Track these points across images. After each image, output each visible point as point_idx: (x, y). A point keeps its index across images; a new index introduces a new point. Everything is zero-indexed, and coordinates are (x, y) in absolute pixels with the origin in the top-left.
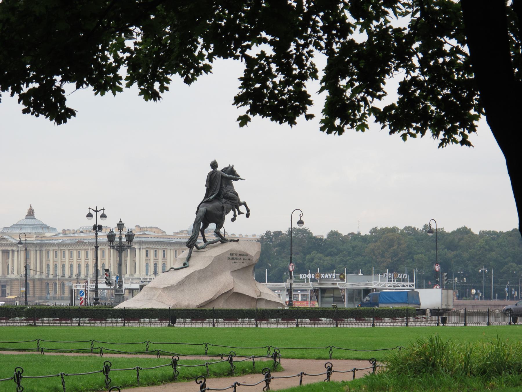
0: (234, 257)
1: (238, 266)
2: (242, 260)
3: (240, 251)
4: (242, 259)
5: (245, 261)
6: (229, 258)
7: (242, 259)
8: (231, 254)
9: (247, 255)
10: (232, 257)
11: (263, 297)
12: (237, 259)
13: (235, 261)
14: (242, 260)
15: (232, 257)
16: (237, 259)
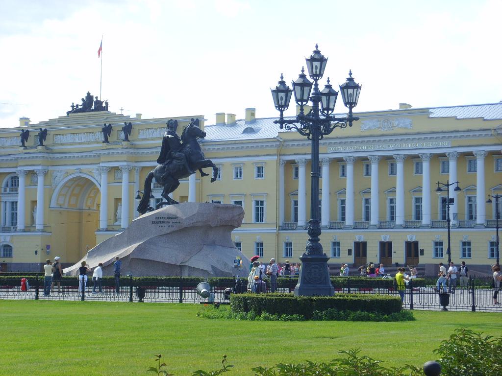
0: (162, 220)
1: (166, 230)
2: (171, 224)
3: (168, 214)
4: (171, 222)
5: (174, 224)
6: (153, 222)
7: (171, 222)
8: (157, 218)
9: (176, 218)
10: (158, 220)
11: (187, 264)
12: (164, 222)
13: (163, 225)
14: (171, 224)
15: (158, 220)
16: (164, 222)
